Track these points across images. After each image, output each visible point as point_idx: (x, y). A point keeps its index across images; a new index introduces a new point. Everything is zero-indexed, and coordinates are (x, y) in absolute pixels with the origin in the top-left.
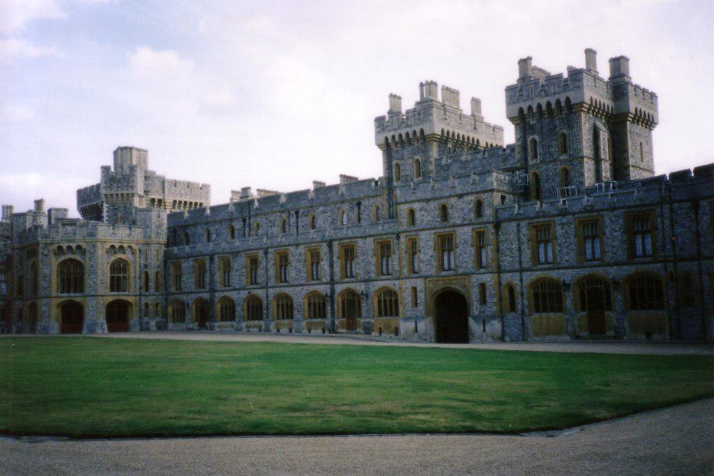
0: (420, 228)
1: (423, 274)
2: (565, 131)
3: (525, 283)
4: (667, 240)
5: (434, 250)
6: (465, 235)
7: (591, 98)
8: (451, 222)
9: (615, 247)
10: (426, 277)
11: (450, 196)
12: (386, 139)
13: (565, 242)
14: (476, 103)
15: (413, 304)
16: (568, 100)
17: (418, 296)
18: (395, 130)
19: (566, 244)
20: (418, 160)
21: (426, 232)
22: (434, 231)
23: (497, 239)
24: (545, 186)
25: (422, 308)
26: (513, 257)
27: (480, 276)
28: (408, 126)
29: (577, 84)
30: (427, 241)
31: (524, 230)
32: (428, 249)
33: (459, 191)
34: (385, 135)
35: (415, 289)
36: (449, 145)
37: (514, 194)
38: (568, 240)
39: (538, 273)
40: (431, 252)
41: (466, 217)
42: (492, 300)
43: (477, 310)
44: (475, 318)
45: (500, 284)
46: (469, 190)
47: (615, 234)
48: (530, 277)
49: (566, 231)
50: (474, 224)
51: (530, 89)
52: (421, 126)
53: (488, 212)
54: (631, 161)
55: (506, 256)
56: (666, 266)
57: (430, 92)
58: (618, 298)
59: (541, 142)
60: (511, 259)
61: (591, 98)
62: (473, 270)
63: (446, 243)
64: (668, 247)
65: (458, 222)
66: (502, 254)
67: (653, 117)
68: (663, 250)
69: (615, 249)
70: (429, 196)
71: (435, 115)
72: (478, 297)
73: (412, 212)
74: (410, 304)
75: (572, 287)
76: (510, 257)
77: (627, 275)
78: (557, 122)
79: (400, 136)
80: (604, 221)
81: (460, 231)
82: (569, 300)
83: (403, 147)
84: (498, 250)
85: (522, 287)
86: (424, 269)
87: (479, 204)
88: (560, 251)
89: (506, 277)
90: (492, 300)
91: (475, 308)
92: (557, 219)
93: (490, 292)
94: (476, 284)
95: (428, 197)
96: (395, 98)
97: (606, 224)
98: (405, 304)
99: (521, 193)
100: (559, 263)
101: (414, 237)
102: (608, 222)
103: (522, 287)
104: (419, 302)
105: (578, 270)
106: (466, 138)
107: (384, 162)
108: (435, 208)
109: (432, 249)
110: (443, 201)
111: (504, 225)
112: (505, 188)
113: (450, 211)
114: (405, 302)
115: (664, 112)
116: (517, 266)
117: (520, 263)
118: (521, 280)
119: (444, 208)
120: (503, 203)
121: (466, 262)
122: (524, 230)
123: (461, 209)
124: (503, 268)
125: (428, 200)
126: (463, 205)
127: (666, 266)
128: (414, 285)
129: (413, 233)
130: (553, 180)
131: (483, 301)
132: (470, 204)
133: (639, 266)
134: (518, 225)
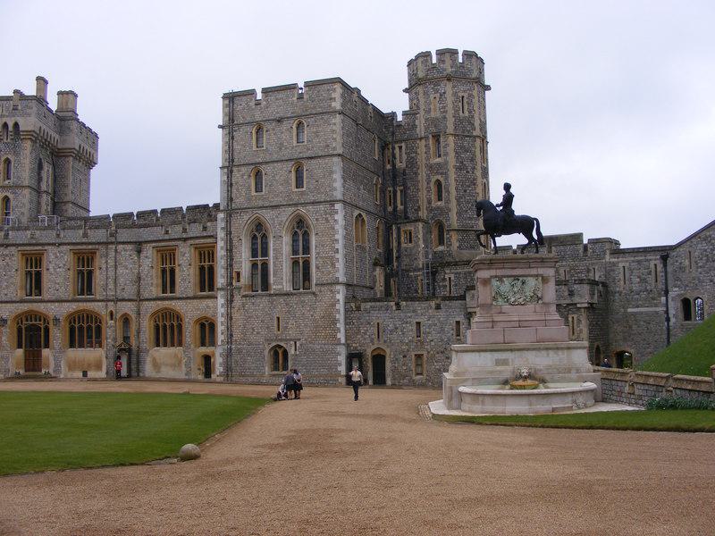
58: (58, 335)
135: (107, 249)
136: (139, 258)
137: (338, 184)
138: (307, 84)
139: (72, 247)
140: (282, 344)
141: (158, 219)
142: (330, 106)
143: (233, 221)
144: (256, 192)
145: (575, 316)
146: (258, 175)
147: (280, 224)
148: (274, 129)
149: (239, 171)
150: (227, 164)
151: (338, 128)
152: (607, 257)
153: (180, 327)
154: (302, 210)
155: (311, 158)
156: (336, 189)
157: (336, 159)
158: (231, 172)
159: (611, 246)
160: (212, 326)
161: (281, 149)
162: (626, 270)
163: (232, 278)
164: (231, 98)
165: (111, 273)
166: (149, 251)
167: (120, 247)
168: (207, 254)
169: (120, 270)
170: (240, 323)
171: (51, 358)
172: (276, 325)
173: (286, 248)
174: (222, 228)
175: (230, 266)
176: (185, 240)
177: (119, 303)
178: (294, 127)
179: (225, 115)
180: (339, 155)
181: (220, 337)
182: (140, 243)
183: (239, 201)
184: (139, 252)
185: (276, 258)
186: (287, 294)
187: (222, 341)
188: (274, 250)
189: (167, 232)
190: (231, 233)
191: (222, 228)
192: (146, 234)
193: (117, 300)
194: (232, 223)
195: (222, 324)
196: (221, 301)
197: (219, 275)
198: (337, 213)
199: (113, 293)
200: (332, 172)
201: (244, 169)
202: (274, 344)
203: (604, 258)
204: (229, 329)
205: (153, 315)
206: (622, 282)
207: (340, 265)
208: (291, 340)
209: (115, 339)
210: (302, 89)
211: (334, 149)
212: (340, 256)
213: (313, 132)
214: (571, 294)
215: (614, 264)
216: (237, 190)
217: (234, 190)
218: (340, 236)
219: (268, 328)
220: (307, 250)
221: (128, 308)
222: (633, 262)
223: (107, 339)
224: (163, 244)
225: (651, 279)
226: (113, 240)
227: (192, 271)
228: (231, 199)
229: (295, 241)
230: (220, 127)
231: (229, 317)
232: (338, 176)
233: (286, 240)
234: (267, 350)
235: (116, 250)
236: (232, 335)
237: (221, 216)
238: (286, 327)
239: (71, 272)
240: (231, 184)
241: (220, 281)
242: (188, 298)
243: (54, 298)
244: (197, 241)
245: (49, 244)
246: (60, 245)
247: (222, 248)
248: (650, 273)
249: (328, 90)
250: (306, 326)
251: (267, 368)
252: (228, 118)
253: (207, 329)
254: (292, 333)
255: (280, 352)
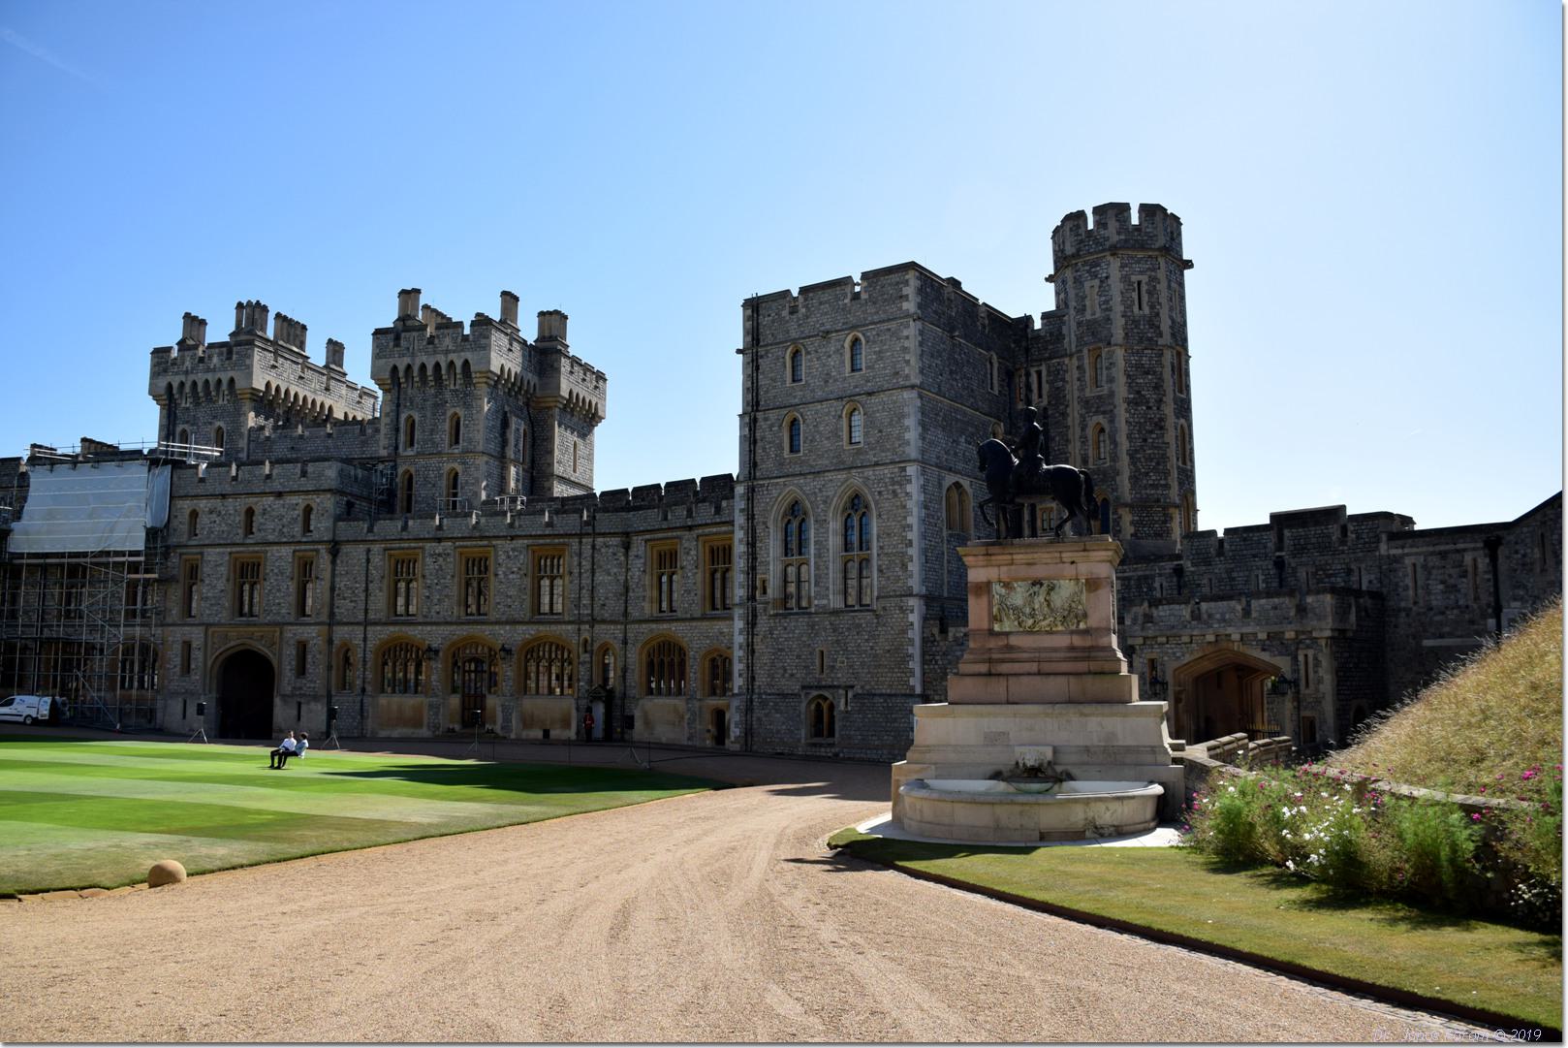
0: (207, 542)
1: (205, 619)
2: (458, 410)
3: (370, 645)
4: (584, 591)
5: (228, 580)
6: (281, 559)
7: (502, 365)
8: (257, 536)
9: (510, 597)
10: (208, 625)
11: (264, 494)
12: (170, 386)
13: (437, 584)
14: (335, 349)
15: (182, 668)
16: (466, 363)
17: (193, 656)
18: (186, 373)
19: (438, 587)
20: (220, 428)
21: (218, 550)
22: (229, 550)
23: (333, 571)
24: (420, 491)
25: (198, 677)
26: (355, 601)
27: (300, 629)
28: (208, 370)
29: (483, 341)
30: (217, 566)
31: (376, 560)
32: (218, 579)
33: (277, 486)
34: (169, 378)
35: (187, 646)
36: (277, 410)
37: (368, 499)
38: (442, 581)
39: (392, 628)
40: (221, 585)
41: (285, 530)
42: (316, 669)
43: (288, 684)
44: (284, 697)
45: (330, 642)
46: (295, 487)
47: (511, 576)
48: (379, 635)
49: (440, 566)
50: (299, 542)
51: (412, 339)
52: (231, 374)
53: (321, 526)
54: (558, 469)
55: (344, 599)
56: (579, 630)
57: (252, 321)
58: (507, 671)
59: (420, 421)
60: (353, 604)
61: (502, 365)
62: (292, 620)
63: (248, 572)
64: (585, 602)
65: (271, 538)
66: (338, 595)
67: (596, 409)
68: (578, 607)
69: (509, 600)
70: (228, 489)
71: (256, 357)
72: (294, 663)
73: (194, 514)
74: (178, 669)
75: (441, 654)
76: (351, 601)
77: (523, 640)
78: (448, 396)
79: (195, 384)
80: (496, 556)
81: (274, 552)
82: (434, 673)
83: (197, 403)
84: (333, 589)
85: (365, 650)
86: (207, 612)
87: (308, 510)
88: (428, 597)
89: (341, 633)
90: (316, 669)
91: (286, 679)
92: (428, 545)
93: (314, 656)
94: (292, 642)
95: (224, 493)
96: (194, 324)
97: (501, 561)
98: (169, 669)
99: (381, 500)
100: (426, 616)
101: (196, 557)
102: (503, 557)
103: (365, 650)
104: (193, 666)
105: (455, 627)
106: (310, 401)
107: (161, 426)
108: (236, 511)
109: (225, 577)
110: (252, 500)
111: (345, 549)
112: (355, 490)
113: (258, 519)
114: (168, 666)
115: (614, 404)
116: (361, 617)
117: (366, 611)
118: (365, 639)
119: (250, 512)
120: (349, 514)
121: (279, 604)
122: (376, 559)
123: (277, 516)
124: (338, 618)
125: (224, 496)
126: (283, 511)
127: (579, 630)
128: (186, 638)
129: (194, 550)
130: (434, 486)
131: (301, 670)
132: (295, 509)
133: (541, 628)
134: (369, 551)
135: (580, 543)
136: (626, 555)
137: (912, 435)
138: (865, 276)
139: (530, 541)
140: (826, 694)
141: (661, 498)
142: (901, 309)
143: (757, 497)
144: (791, 451)
145: (1310, 653)
146: (794, 423)
147: (825, 502)
148: (816, 352)
149: (766, 419)
150: (750, 409)
151: (912, 344)
152: (1383, 548)
153: (682, 663)
154: (856, 480)
155: (870, 394)
156: (908, 443)
157: (906, 394)
158: (755, 420)
159: (1392, 527)
160: (727, 661)
161: (827, 382)
162: (1419, 569)
163: (754, 588)
164: (754, 307)
165: (586, 581)
166: (638, 545)
167: (600, 540)
168: (720, 555)
169: (600, 577)
170: (765, 659)
171: (499, 709)
172: (818, 671)
173: (834, 541)
174: (741, 511)
175: (752, 570)
176: (690, 528)
177: (597, 627)
178: (847, 344)
179: (746, 333)
180: (913, 387)
181: (738, 682)
182: (627, 534)
183: (766, 466)
184: (627, 547)
185: (818, 556)
186: (836, 612)
187: (740, 687)
188: (816, 543)
189: (665, 518)
190: (753, 515)
191: (741, 511)
192: (636, 520)
193: (593, 621)
194: (755, 501)
195: (740, 661)
196: (739, 624)
197: (736, 584)
198: (909, 481)
199: (589, 612)
200: (902, 416)
201: (773, 415)
202: (815, 693)
203: (1377, 548)
204: (750, 668)
205: (646, 643)
206: (1411, 592)
207: (914, 567)
208: (838, 687)
209: (590, 682)
210: (858, 284)
211: (907, 377)
212: (913, 551)
213: (875, 352)
214: (1302, 610)
215: (1397, 559)
216: (764, 449)
217: (759, 451)
218: (913, 520)
219: (806, 667)
220: (864, 544)
221: (610, 633)
222: (1432, 554)
223: (579, 680)
224: (660, 535)
225: (1465, 585)
226: (590, 531)
227: (699, 577)
228: (755, 465)
229: (847, 528)
230: (739, 351)
231: (750, 649)
232: (911, 422)
233: (835, 525)
234: (804, 705)
235: (593, 547)
236: (753, 678)
237: (740, 490)
238: (833, 667)
239: (529, 579)
240: (755, 442)
241: (738, 592)
242: (693, 619)
243: (504, 618)
244: (707, 530)
245: (497, 537)
246: (513, 538)
247: (741, 541)
248: (1464, 574)
249: (898, 283)
250: (863, 664)
251: (803, 732)
252: (749, 338)
253: (719, 669)
254: (842, 677)
255: (825, 706)
